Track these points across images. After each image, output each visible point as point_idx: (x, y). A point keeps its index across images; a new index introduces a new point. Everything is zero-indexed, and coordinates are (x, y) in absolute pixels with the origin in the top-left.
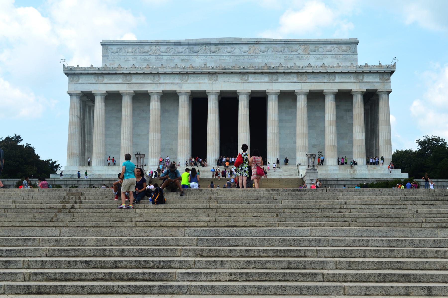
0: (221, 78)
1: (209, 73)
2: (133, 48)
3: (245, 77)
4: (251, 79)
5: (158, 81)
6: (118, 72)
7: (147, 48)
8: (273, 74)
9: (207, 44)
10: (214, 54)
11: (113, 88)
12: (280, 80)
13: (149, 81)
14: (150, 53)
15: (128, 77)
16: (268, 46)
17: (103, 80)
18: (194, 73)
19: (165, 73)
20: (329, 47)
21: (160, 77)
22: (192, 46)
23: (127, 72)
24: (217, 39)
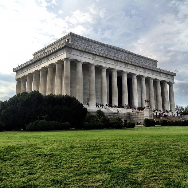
0: (129, 66)
1: (126, 63)
2: (85, 42)
3: (136, 68)
4: (139, 69)
5: (107, 61)
6: (92, 52)
7: (91, 43)
8: (145, 68)
9: (114, 48)
10: (116, 54)
11: (88, 61)
12: (146, 72)
13: (103, 61)
14: (92, 46)
15: (95, 56)
16: (133, 56)
17: (83, 55)
18: (121, 62)
19: (111, 59)
20: (150, 62)
21: (107, 60)
22: (108, 48)
23: (95, 53)
24: (117, 47)
